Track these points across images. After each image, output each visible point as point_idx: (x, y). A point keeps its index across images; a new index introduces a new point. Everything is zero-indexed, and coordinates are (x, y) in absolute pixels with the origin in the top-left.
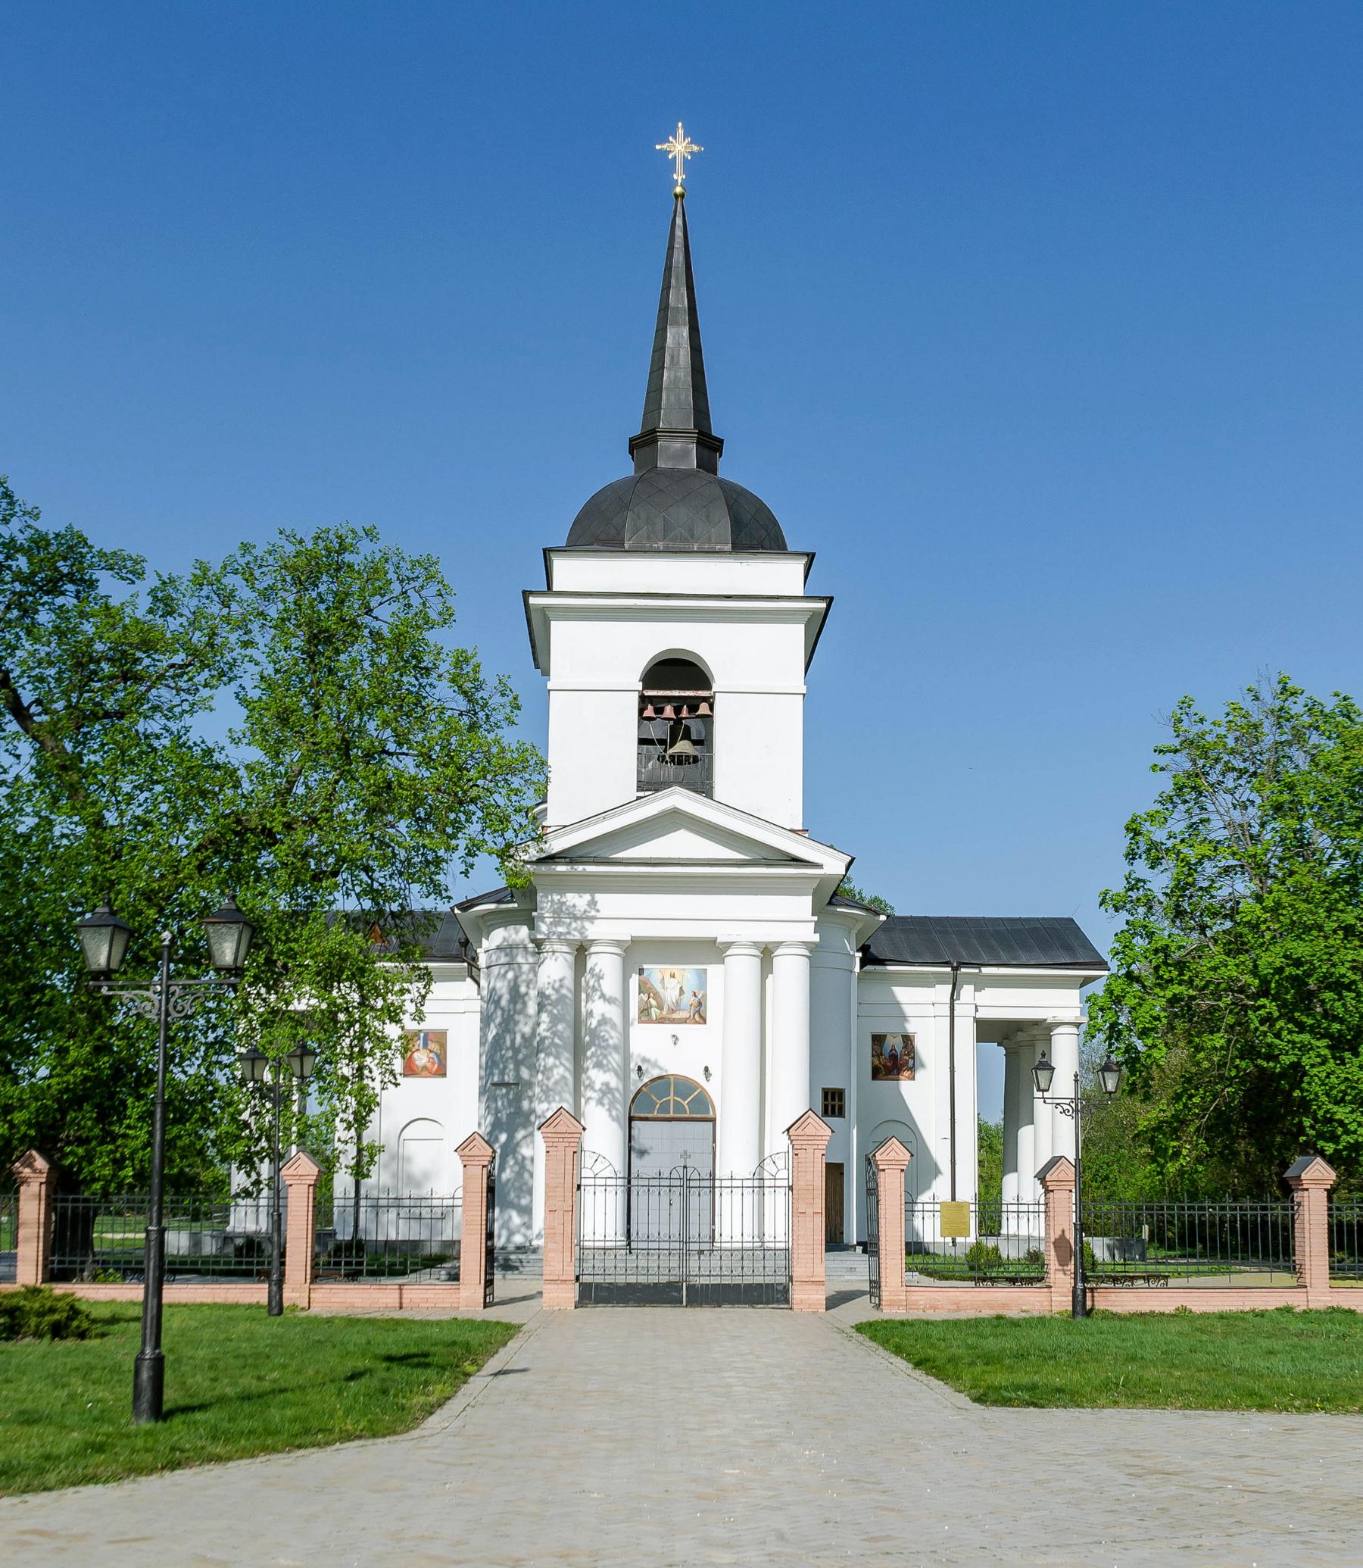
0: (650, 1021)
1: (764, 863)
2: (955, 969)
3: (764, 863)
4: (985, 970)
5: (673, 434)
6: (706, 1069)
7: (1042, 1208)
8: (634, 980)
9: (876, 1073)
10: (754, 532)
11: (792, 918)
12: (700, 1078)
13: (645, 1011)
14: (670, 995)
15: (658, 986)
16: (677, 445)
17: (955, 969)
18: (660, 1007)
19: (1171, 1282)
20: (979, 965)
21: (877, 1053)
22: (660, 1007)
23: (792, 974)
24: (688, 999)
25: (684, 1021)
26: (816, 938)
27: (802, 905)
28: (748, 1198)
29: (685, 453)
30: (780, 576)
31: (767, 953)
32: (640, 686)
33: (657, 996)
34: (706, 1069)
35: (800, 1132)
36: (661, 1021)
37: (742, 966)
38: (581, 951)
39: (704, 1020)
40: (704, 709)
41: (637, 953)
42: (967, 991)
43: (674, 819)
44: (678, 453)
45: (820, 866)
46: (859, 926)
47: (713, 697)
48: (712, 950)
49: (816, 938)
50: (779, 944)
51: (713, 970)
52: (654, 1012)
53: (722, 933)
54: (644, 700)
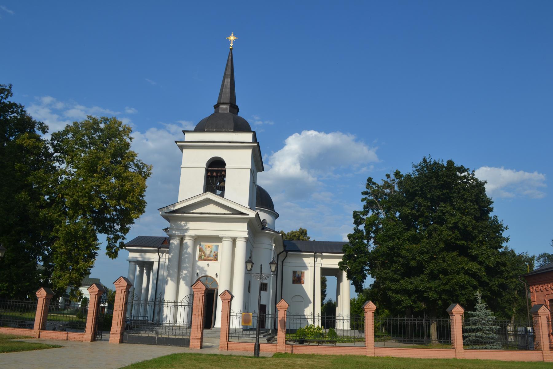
0: (202, 260)
1: (235, 215)
2: (315, 253)
3: (235, 215)
4: (324, 254)
5: (224, 104)
6: (217, 274)
7: (232, 314)
8: (198, 248)
9: (294, 282)
10: (241, 126)
11: (241, 230)
12: (214, 277)
13: (200, 258)
14: (208, 252)
15: (204, 249)
16: (225, 107)
17: (315, 253)
18: (205, 256)
19: (338, 344)
20: (322, 253)
21: (294, 276)
22: (205, 256)
23: (241, 247)
24: (213, 254)
25: (211, 260)
26: (247, 236)
27: (244, 226)
28: (172, 309)
29: (227, 109)
30: (247, 137)
31: (234, 240)
32: (205, 167)
33: (204, 253)
34: (217, 274)
35: (196, 287)
36: (205, 260)
37: (226, 246)
38: (182, 239)
39: (217, 260)
40: (223, 173)
41: (198, 239)
42: (319, 259)
43: (208, 202)
44: (225, 108)
45: (248, 215)
46: (274, 237)
47: (225, 171)
48: (218, 239)
49: (247, 236)
50: (237, 237)
51: (220, 244)
52: (203, 257)
53: (221, 234)
54: (207, 171)
